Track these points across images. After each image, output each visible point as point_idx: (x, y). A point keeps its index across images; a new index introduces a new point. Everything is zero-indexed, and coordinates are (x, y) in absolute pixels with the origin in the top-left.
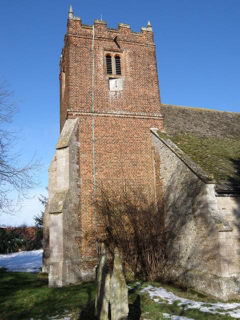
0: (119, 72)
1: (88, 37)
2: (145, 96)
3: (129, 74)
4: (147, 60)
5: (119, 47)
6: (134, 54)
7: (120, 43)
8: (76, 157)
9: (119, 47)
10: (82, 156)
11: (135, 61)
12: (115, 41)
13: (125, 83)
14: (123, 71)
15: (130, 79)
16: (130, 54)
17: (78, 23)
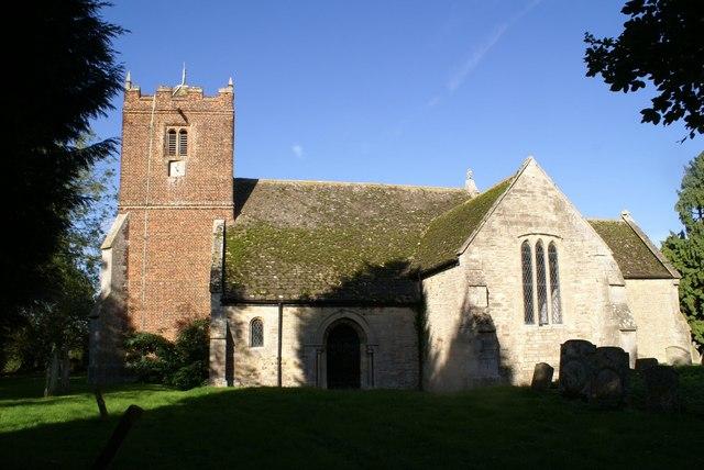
0: (184, 152)
1: (146, 110)
2: (214, 180)
3: (195, 154)
4: (221, 132)
5: (186, 119)
6: (204, 128)
7: (187, 114)
8: (123, 258)
9: (186, 119)
10: (131, 255)
11: (204, 136)
12: (180, 112)
13: (188, 166)
14: (189, 150)
15: (196, 160)
16: (199, 128)
17: (136, 94)
